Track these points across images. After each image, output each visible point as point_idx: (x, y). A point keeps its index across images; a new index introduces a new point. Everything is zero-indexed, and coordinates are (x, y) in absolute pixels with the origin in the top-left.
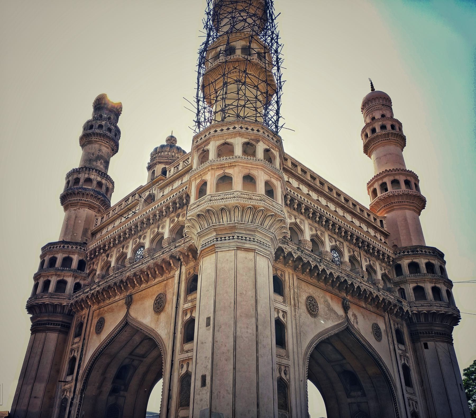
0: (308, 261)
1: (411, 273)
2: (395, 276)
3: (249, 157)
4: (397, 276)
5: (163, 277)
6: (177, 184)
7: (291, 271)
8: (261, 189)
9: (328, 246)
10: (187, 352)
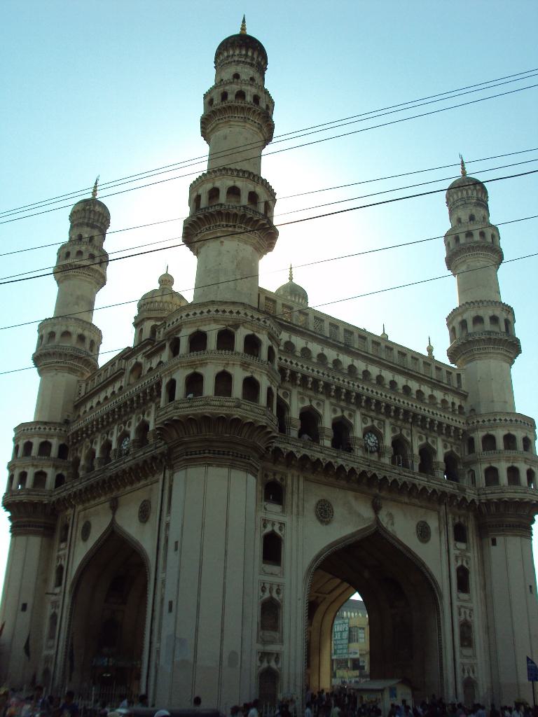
0: (318, 459)
2: (466, 454)
5: (148, 481)
7: (296, 473)
8: (237, 389)
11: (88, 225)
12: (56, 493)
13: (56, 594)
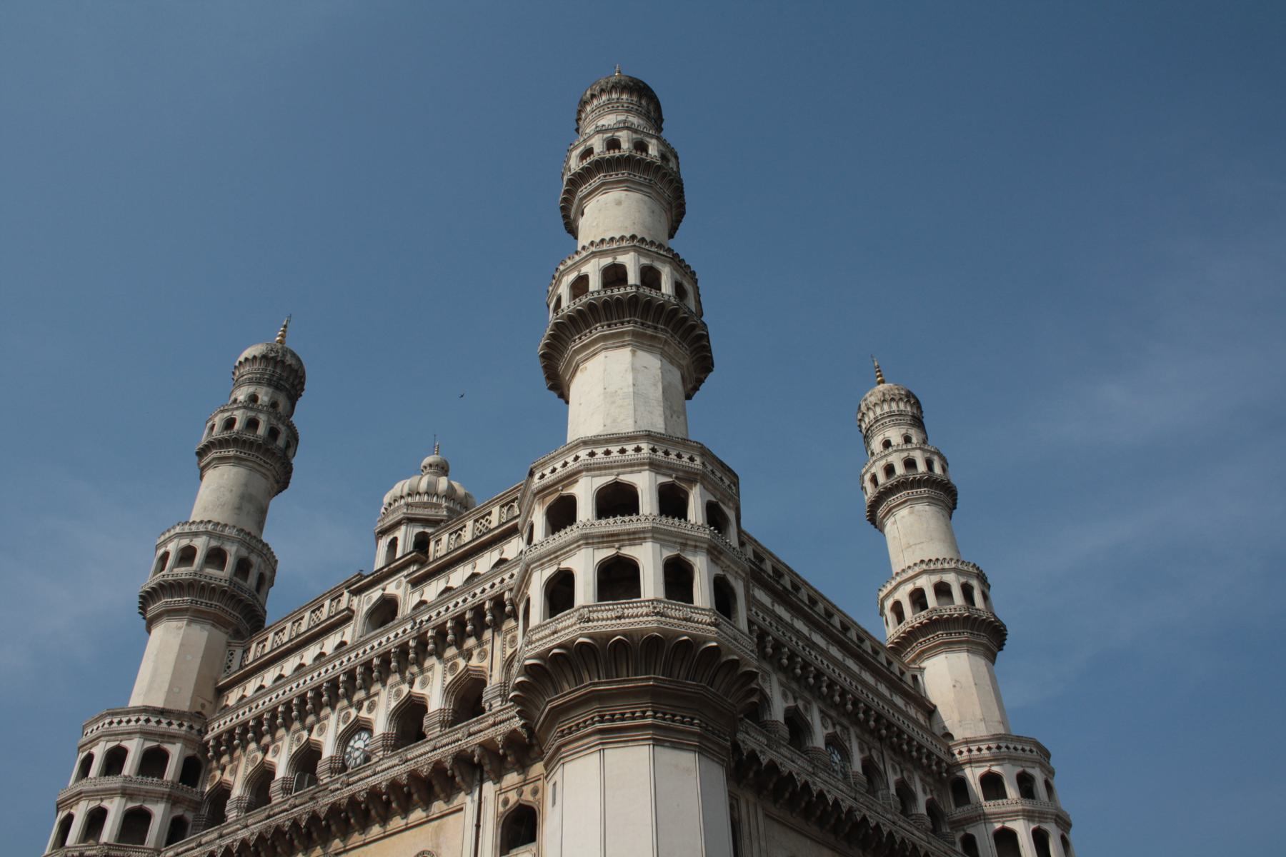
0: (790, 773)
1: (986, 798)
4: (957, 806)
6: (457, 577)
9: (818, 739)
11: (270, 383)
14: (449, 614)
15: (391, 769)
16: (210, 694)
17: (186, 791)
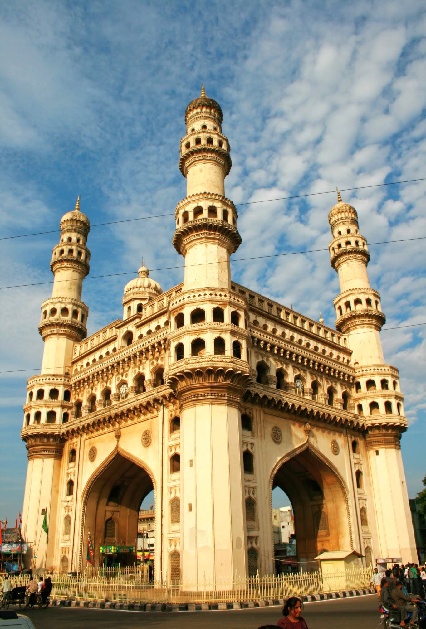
0: (273, 399)
3: (218, 323)
10: (175, 481)
12: (65, 426)
13: (68, 501)
14: (150, 344)
15: (134, 400)
16: (70, 365)
17: (66, 403)
